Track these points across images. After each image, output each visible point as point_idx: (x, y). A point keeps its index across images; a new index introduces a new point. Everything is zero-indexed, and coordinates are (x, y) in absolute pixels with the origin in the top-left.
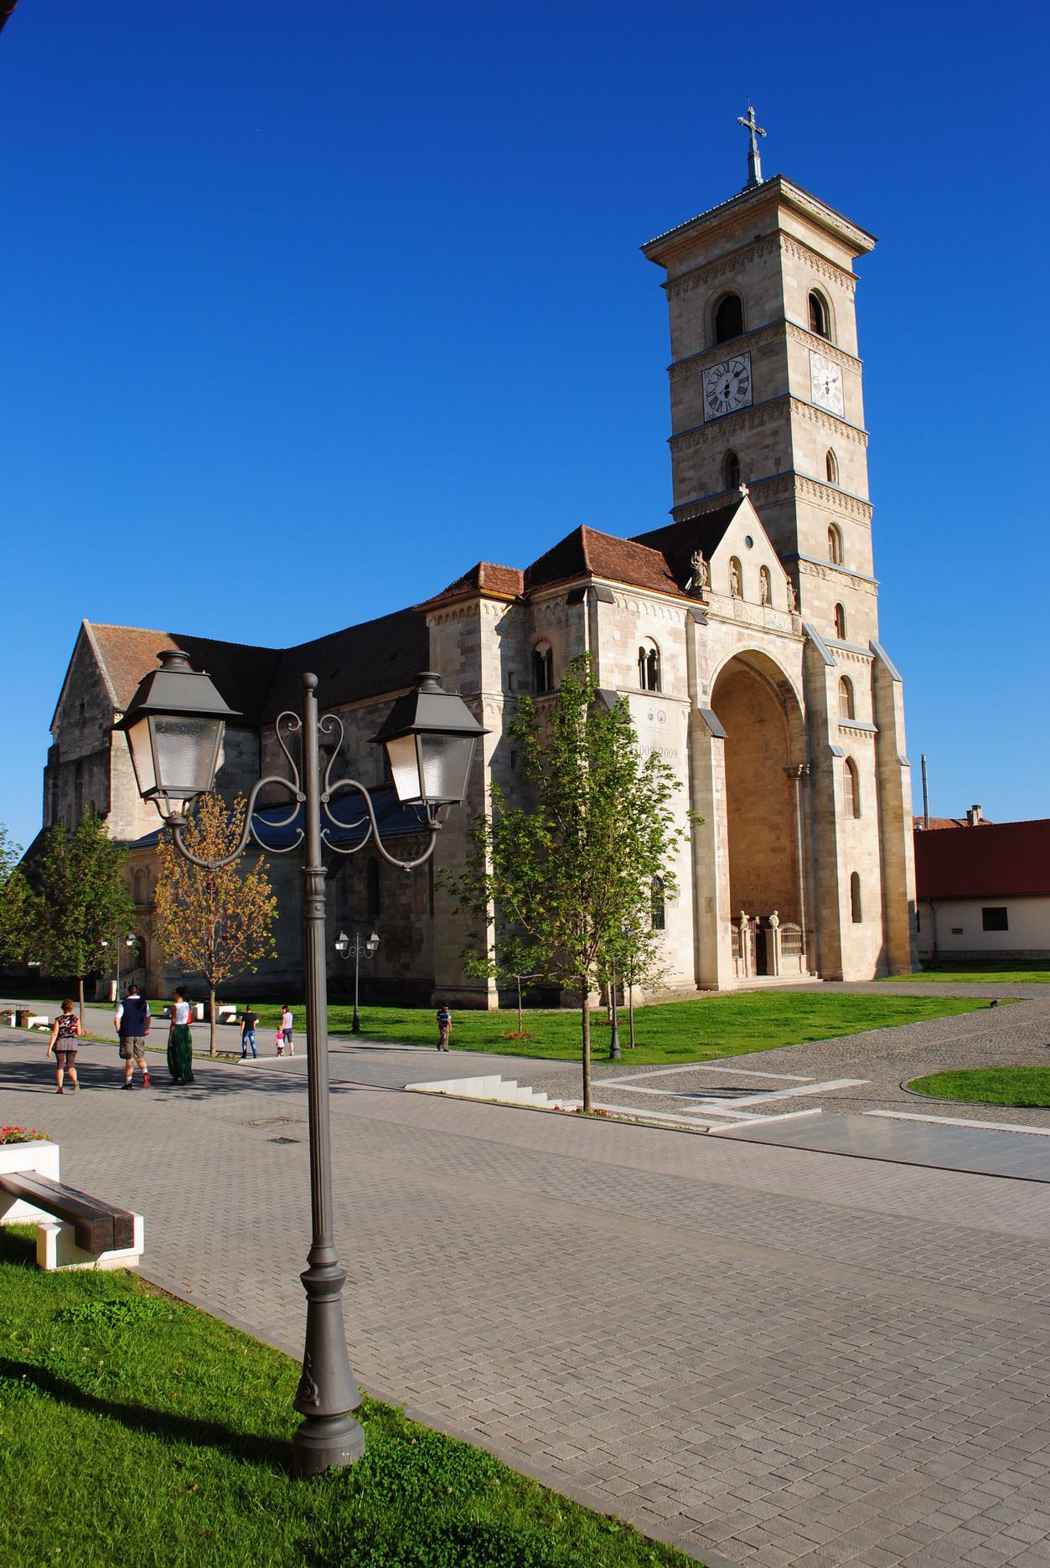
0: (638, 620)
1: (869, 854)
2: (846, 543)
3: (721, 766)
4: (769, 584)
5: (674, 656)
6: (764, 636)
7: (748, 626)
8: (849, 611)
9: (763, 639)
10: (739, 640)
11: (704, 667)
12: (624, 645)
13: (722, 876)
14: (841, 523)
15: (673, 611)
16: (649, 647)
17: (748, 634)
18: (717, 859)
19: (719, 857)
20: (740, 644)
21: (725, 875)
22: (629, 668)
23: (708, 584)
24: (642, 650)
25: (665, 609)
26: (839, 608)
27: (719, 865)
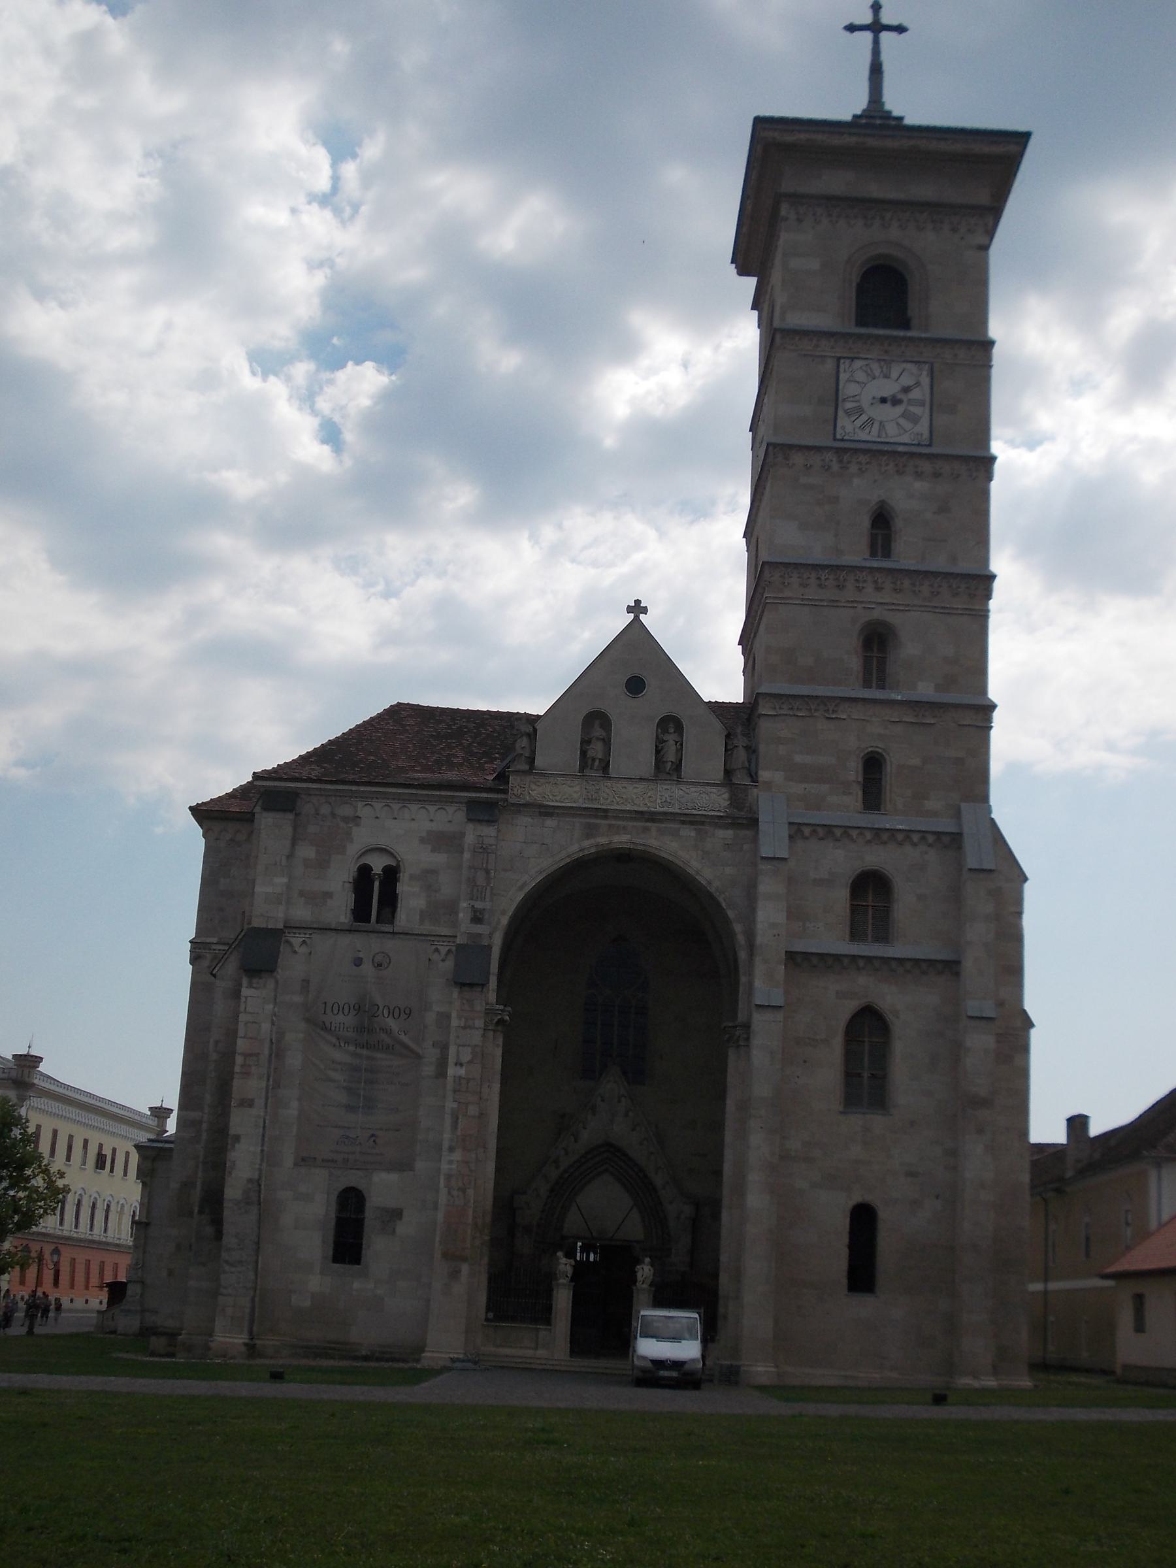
0: (355, 829)
1: (911, 1174)
2: (908, 649)
3: (471, 1028)
4: (680, 744)
5: (427, 876)
6: (648, 824)
7: (605, 813)
8: (898, 758)
9: (646, 829)
10: (588, 836)
11: (481, 879)
12: (322, 864)
13: (455, 1193)
14: (894, 619)
15: (432, 809)
16: (378, 864)
17: (610, 826)
18: (445, 1167)
19: (450, 1162)
20: (586, 843)
21: (463, 1190)
22: (328, 895)
23: (531, 761)
24: (364, 872)
25: (414, 807)
26: (873, 764)
27: (449, 1177)
